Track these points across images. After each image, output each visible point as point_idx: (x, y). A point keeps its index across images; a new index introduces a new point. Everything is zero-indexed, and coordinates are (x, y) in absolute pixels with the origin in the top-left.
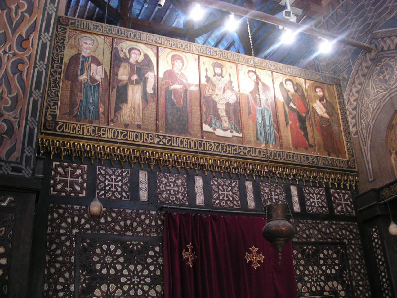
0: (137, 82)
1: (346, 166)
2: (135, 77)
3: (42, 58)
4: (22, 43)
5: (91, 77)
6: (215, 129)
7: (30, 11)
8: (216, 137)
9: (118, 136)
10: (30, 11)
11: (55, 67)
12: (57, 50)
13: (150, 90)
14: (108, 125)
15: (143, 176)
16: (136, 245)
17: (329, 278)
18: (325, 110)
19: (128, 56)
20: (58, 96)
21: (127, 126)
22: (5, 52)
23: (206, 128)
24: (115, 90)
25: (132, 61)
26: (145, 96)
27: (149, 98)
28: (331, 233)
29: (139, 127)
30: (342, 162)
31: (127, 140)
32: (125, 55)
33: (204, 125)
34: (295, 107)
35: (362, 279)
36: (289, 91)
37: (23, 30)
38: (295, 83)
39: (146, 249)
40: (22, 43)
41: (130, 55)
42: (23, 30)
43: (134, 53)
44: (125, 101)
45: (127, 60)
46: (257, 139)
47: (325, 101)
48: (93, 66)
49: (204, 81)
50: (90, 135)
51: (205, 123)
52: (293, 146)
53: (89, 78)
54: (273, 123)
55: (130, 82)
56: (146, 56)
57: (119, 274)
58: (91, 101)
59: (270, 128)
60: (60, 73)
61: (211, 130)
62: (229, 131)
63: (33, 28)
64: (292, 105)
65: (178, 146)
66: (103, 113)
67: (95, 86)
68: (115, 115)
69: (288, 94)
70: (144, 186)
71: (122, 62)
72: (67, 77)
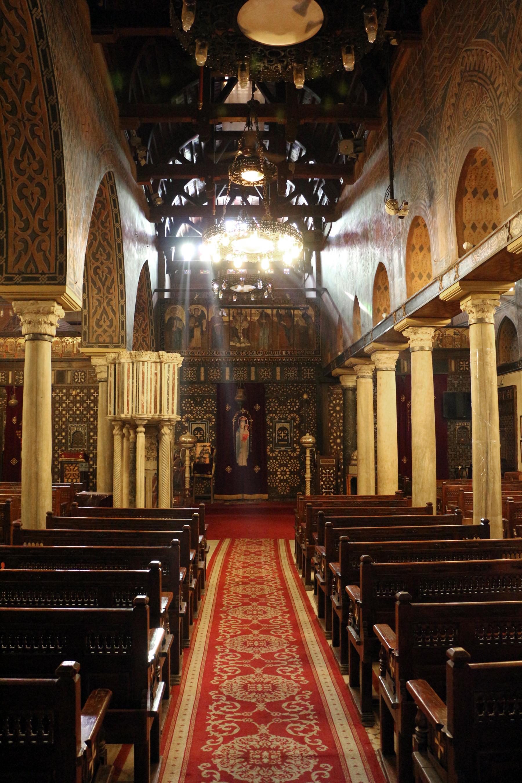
0: (198, 326)
2: (197, 324)
3: (152, 334)
4: (144, 331)
7: (144, 319)
10: (144, 319)
13: (204, 329)
15: (202, 369)
16: (199, 399)
17: (291, 412)
18: (304, 321)
21: (194, 348)
23: (232, 344)
25: (195, 316)
26: (202, 333)
28: (297, 390)
29: (200, 348)
35: (312, 413)
37: (143, 327)
39: (203, 400)
40: (144, 331)
42: (143, 327)
48: (178, 322)
49: (231, 318)
55: (195, 326)
56: (202, 311)
57: (192, 410)
61: (234, 344)
63: (146, 326)
70: (202, 374)
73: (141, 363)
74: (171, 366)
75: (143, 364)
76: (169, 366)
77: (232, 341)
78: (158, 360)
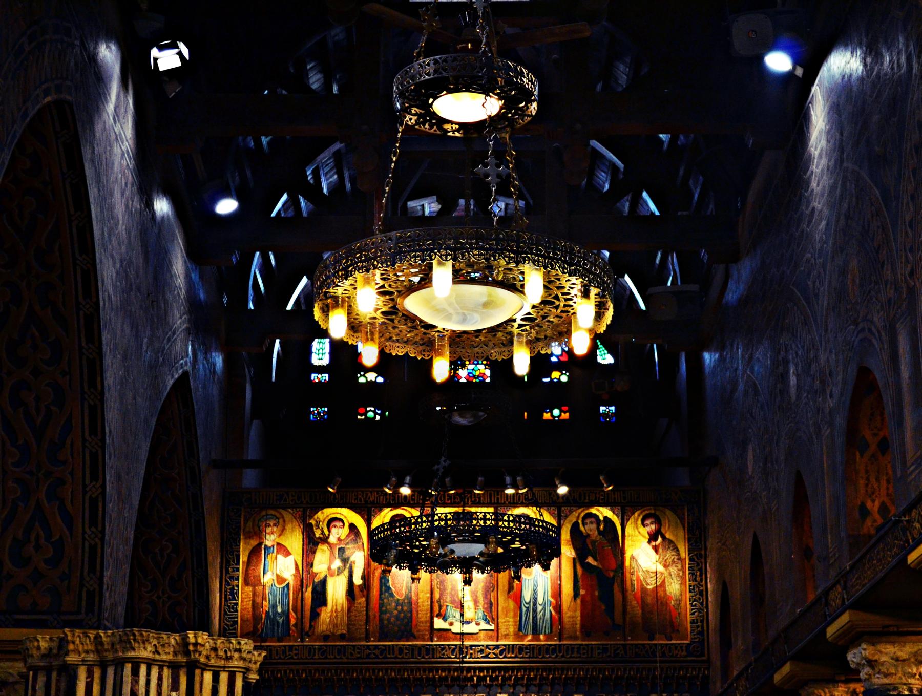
1: (684, 653)
5: (278, 576)
6: (451, 624)
8: (451, 635)
9: (314, 655)
11: (230, 570)
12: (231, 546)
13: (358, 581)
14: (302, 641)
19: (327, 532)
20: (237, 611)
21: (326, 638)
22: (159, 597)
23: (439, 624)
24: (310, 589)
27: (356, 591)
29: (342, 637)
30: (676, 648)
31: (326, 658)
32: (323, 533)
33: (436, 619)
34: (595, 563)
36: (588, 535)
38: (601, 518)
41: (329, 531)
43: (335, 526)
44: (325, 603)
45: (325, 540)
46: (520, 629)
47: (660, 539)
50: (280, 658)
51: (437, 616)
52: (581, 632)
53: (275, 579)
54: (550, 598)
56: (353, 527)
58: (279, 610)
59: (544, 609)
60: (238, 579)
61: (445, 626)
62: (474, 623)
64: (590, 560)
65: (396, 658)
66: (295, 625)
67: (284, 588)
68: (311, 626)
69: (585, 542)
71: (316, 544)
72: (246, 583)
73: (128, 667)
74: (224, 677)
75: (135, 673)
76: (216, 679)
77: (439, 616)
78: (181, 659)
